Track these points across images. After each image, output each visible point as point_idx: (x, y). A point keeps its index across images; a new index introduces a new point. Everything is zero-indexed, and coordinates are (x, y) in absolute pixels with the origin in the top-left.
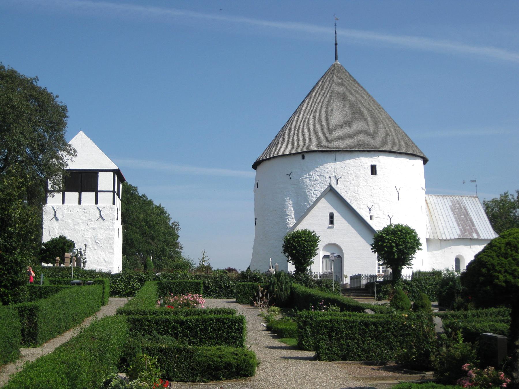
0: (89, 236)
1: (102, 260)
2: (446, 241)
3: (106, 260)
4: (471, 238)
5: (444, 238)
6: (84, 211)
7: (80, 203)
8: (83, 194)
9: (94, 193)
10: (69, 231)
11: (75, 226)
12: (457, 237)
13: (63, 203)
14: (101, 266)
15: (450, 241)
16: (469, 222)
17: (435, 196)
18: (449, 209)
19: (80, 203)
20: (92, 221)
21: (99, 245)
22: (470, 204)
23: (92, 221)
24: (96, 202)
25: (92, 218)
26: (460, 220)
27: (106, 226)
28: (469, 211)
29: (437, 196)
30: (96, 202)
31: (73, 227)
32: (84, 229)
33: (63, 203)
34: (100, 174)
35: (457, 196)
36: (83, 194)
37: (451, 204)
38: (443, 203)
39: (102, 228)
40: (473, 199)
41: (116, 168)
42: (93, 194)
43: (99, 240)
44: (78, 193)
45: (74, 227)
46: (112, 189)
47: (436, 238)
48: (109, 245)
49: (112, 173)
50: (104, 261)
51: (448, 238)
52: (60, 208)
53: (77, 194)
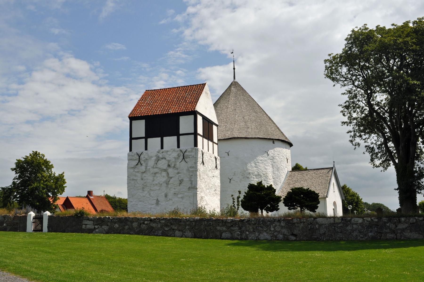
8: (165, 138)
9: (175, 138)
13: (146, 149)
24: (178, 146)
30: (178, 146)
33: (146, 149)
36: (165, 138)
42: (175, 138)
44: (159, 139)
53: (159, 139)
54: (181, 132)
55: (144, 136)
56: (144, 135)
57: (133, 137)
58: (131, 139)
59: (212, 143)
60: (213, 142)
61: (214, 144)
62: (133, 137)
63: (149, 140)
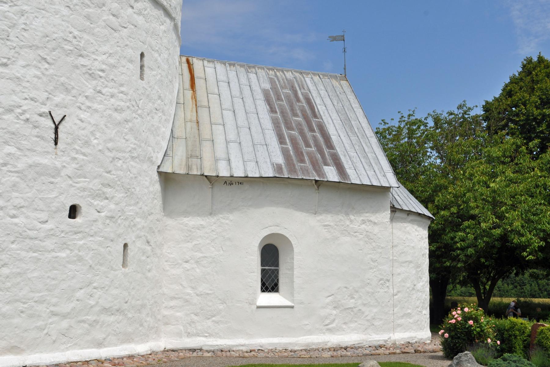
2: (231, 184)
4: (317, 179)
5: (224, 173)
12: (269, 173)
15: (246, 186)
16: (318, 135)
17: (225, 64)
18: (260, 96)
22: (323, 93)
26: (289, 127)
28: (320, 108)
29: (230, 65)
35: (287, 71)
37: (267, 86)
38: (244, 80)
40: (334, 82)
47: (195, 172)
51: (239, 173)
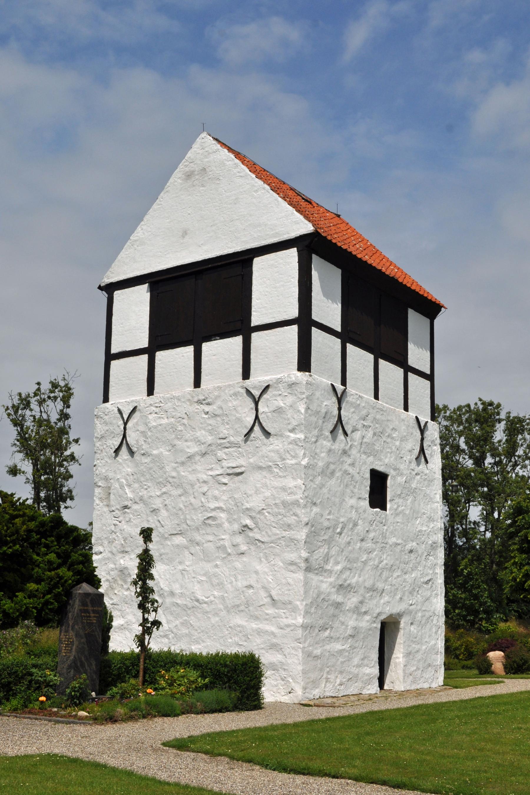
0: (222, 505)
1: (263, 594)
3: (276, 598)
6: (207, 408)
7: (197, 383)
8: (206, 346)
10: (164, 490)
11: (181, 469)
13: (150, 391)
14: (257, 618)
19: (197, 383)
20: (233, 445)
21: (251, 534)
23: (233, 445)
24: (246, 374)
25: (232, 432)
27: (276, 457)
30: (246, 374)
31: (174, 474)
32: (205, 477)
33: (150, 391)
34: (258, 263)
36: (206, 346)
39: (260, 468)
41: (307, 228)
42: (238, 340)
43: (253, 514)
45: (178, 472)
46: (294, 312)
48: (285, 534)
49: (293, 253)
50: (269, 600)
52: (139, 410)
53: (190, 350)
54: (256, 320)
55: (146, 345)
56: (144, 342)
57: (114, 350)
58: (110, 357)
59: (400, 372)
60: (408, 369)
61: (411, 376)
62: (114, 350)
63: (160, 355)
